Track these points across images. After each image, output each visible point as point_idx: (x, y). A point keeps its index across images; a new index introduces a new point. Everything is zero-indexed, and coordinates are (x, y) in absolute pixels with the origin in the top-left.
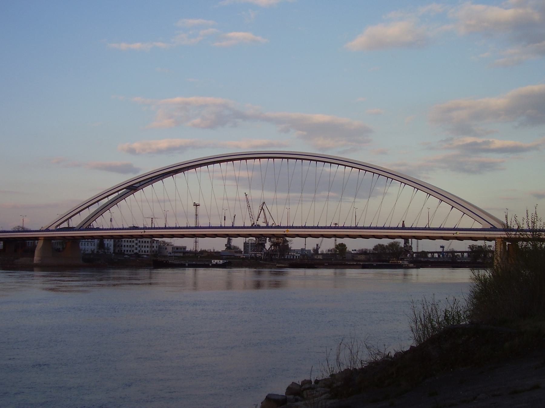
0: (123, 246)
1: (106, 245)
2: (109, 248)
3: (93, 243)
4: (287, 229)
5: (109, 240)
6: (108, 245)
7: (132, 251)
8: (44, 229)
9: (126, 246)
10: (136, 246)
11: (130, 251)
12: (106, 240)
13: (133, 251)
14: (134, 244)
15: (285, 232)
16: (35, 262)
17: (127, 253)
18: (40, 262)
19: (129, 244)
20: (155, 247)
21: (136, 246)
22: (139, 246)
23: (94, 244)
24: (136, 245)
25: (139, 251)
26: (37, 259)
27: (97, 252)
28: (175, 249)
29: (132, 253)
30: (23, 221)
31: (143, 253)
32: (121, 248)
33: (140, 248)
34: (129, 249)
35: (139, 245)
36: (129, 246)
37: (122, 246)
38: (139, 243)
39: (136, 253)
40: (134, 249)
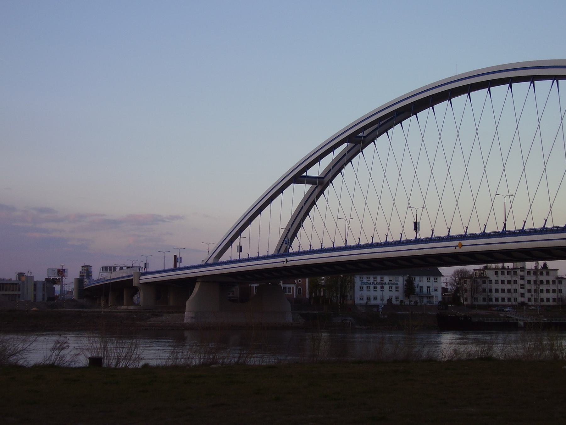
0: (494, 291)
1: (425, 290)
2: (431, 294)
3: (394, 287)
4: (459, 241)
5: (432, 279)
7: (513, 300)
8: (204, 263)
9: (500, 290)
10: (522, 291)
11: (509, 299)
13: (515, 299)
14: (517, 287)
15: (457, 247)
16: (185, 321)
17: (510, 303)
18: (194, 320)
19: (506, 287)
21: (522, 291)
22: (529, 291)
23: (397, 288)
24: (521, 288)
25: (529, 299)
26: (188, 316)
27: (401, 301)
29: (514, 303)
30: (208, 252)
31: (506, 303)
32: (489, 294)
33: (530, 294)
34: (506, 295)
35: (529, 288)
36: (506, 291)
37: (491, 291)
38: (529, 285)
39: (523, 304)
40: (515, 295)
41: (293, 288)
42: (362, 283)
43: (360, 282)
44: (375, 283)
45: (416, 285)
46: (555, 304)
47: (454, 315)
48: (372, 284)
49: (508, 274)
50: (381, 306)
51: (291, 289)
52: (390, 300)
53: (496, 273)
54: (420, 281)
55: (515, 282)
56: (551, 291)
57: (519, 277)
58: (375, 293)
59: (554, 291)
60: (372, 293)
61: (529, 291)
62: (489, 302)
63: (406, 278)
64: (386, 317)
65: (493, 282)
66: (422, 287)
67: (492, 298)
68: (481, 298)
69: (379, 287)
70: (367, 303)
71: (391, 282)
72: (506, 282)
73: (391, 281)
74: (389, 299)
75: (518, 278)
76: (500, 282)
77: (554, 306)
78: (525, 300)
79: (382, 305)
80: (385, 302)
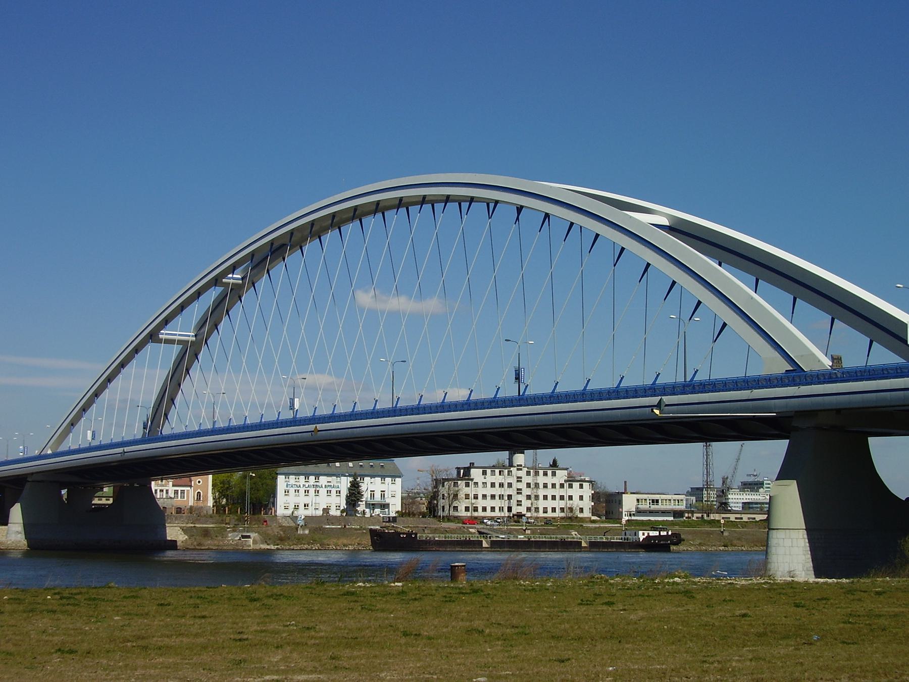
0: (480, 497)
2: (385, 502)
3: (334, 491)
5: (388, 480)
6: (383, 496)
10: (520, 497)
11: (501, 509)
12: (367, 479)
13: (510, 509)
19: (497, 491)
20: (576, 498)
21: (520, 497)
22: (529, 497)
25: (529, 509)
28: (648, 501)
31: (489, 513)
32: (474, 501)
33: (530, 501)
34: (497, 503)
39: (520, 515)
41: (187, 490)
42: (287, 486)
43: (286, 484)
44: (307, 486)
45: (363, 487)
46: (563, 515)
47: (393, 531)
48: (302, 486)
49: (500, 474)
50: (301, 518)
51: (184, 493)
52: (326, 510)
53: (484, 473)
54: (371, 483)
55: (510, 485)
56: (558, 498)
57: (515, 478)
58: (307, 500)
59: (562, 498)
60: (302, 500)
61: (529, 497)
62: (473, 513)
63: (350, 479)
64: (307, 532)
65: (480, 484)
66: (374, 491)
67: (477, 507)
68: (462, 508)
69: (312, 490)
70: (293, 513)
71: (329, 484)
72: (497, 485)
73: (330, 482)
74: (326, 507)
75: (513, 480)
76: (489, 485)
77: (562, 518)
78: (522, 510)
79: (303, 516)
80: (320, 513)
